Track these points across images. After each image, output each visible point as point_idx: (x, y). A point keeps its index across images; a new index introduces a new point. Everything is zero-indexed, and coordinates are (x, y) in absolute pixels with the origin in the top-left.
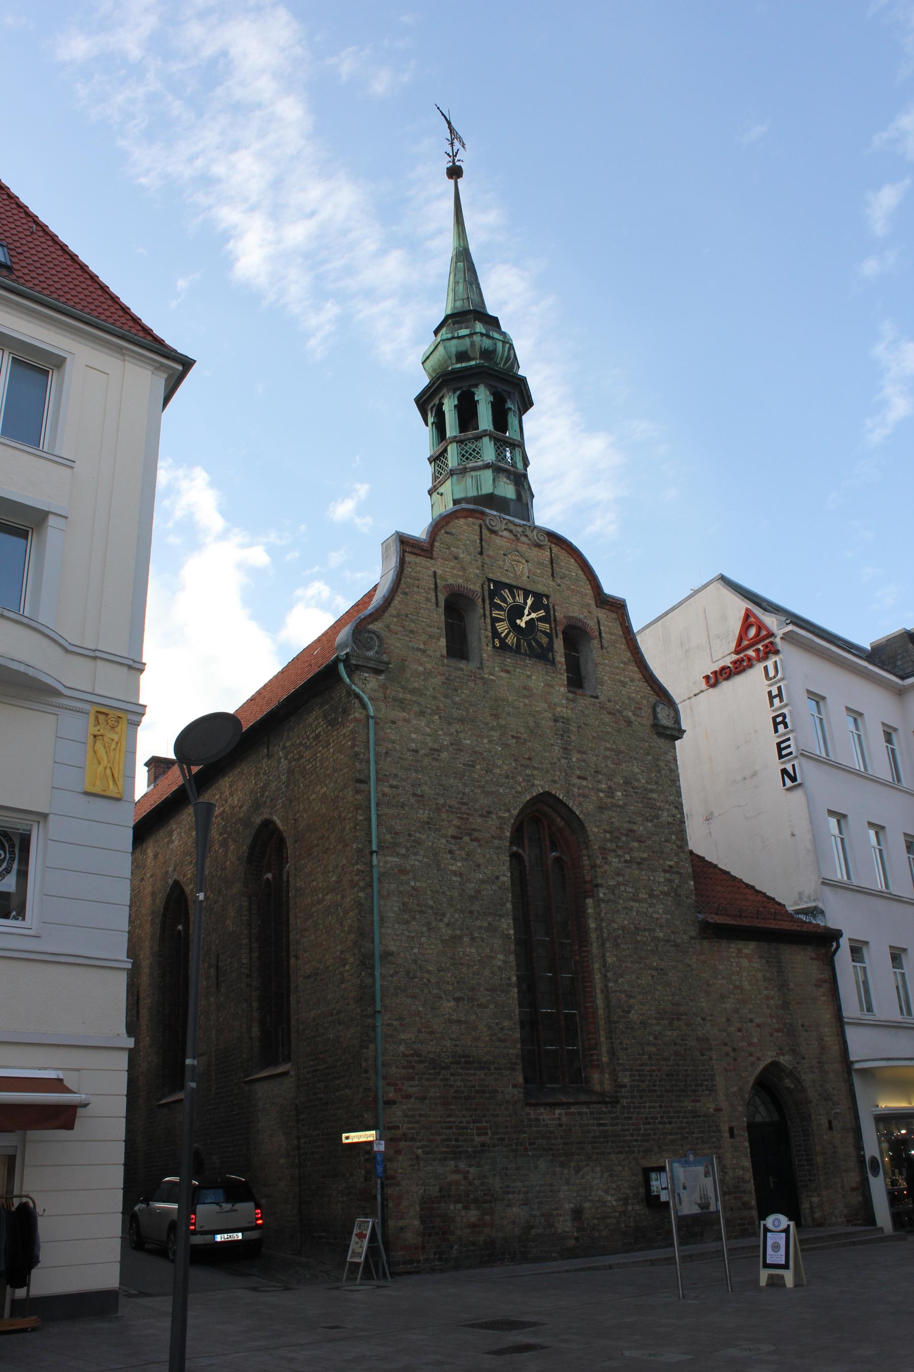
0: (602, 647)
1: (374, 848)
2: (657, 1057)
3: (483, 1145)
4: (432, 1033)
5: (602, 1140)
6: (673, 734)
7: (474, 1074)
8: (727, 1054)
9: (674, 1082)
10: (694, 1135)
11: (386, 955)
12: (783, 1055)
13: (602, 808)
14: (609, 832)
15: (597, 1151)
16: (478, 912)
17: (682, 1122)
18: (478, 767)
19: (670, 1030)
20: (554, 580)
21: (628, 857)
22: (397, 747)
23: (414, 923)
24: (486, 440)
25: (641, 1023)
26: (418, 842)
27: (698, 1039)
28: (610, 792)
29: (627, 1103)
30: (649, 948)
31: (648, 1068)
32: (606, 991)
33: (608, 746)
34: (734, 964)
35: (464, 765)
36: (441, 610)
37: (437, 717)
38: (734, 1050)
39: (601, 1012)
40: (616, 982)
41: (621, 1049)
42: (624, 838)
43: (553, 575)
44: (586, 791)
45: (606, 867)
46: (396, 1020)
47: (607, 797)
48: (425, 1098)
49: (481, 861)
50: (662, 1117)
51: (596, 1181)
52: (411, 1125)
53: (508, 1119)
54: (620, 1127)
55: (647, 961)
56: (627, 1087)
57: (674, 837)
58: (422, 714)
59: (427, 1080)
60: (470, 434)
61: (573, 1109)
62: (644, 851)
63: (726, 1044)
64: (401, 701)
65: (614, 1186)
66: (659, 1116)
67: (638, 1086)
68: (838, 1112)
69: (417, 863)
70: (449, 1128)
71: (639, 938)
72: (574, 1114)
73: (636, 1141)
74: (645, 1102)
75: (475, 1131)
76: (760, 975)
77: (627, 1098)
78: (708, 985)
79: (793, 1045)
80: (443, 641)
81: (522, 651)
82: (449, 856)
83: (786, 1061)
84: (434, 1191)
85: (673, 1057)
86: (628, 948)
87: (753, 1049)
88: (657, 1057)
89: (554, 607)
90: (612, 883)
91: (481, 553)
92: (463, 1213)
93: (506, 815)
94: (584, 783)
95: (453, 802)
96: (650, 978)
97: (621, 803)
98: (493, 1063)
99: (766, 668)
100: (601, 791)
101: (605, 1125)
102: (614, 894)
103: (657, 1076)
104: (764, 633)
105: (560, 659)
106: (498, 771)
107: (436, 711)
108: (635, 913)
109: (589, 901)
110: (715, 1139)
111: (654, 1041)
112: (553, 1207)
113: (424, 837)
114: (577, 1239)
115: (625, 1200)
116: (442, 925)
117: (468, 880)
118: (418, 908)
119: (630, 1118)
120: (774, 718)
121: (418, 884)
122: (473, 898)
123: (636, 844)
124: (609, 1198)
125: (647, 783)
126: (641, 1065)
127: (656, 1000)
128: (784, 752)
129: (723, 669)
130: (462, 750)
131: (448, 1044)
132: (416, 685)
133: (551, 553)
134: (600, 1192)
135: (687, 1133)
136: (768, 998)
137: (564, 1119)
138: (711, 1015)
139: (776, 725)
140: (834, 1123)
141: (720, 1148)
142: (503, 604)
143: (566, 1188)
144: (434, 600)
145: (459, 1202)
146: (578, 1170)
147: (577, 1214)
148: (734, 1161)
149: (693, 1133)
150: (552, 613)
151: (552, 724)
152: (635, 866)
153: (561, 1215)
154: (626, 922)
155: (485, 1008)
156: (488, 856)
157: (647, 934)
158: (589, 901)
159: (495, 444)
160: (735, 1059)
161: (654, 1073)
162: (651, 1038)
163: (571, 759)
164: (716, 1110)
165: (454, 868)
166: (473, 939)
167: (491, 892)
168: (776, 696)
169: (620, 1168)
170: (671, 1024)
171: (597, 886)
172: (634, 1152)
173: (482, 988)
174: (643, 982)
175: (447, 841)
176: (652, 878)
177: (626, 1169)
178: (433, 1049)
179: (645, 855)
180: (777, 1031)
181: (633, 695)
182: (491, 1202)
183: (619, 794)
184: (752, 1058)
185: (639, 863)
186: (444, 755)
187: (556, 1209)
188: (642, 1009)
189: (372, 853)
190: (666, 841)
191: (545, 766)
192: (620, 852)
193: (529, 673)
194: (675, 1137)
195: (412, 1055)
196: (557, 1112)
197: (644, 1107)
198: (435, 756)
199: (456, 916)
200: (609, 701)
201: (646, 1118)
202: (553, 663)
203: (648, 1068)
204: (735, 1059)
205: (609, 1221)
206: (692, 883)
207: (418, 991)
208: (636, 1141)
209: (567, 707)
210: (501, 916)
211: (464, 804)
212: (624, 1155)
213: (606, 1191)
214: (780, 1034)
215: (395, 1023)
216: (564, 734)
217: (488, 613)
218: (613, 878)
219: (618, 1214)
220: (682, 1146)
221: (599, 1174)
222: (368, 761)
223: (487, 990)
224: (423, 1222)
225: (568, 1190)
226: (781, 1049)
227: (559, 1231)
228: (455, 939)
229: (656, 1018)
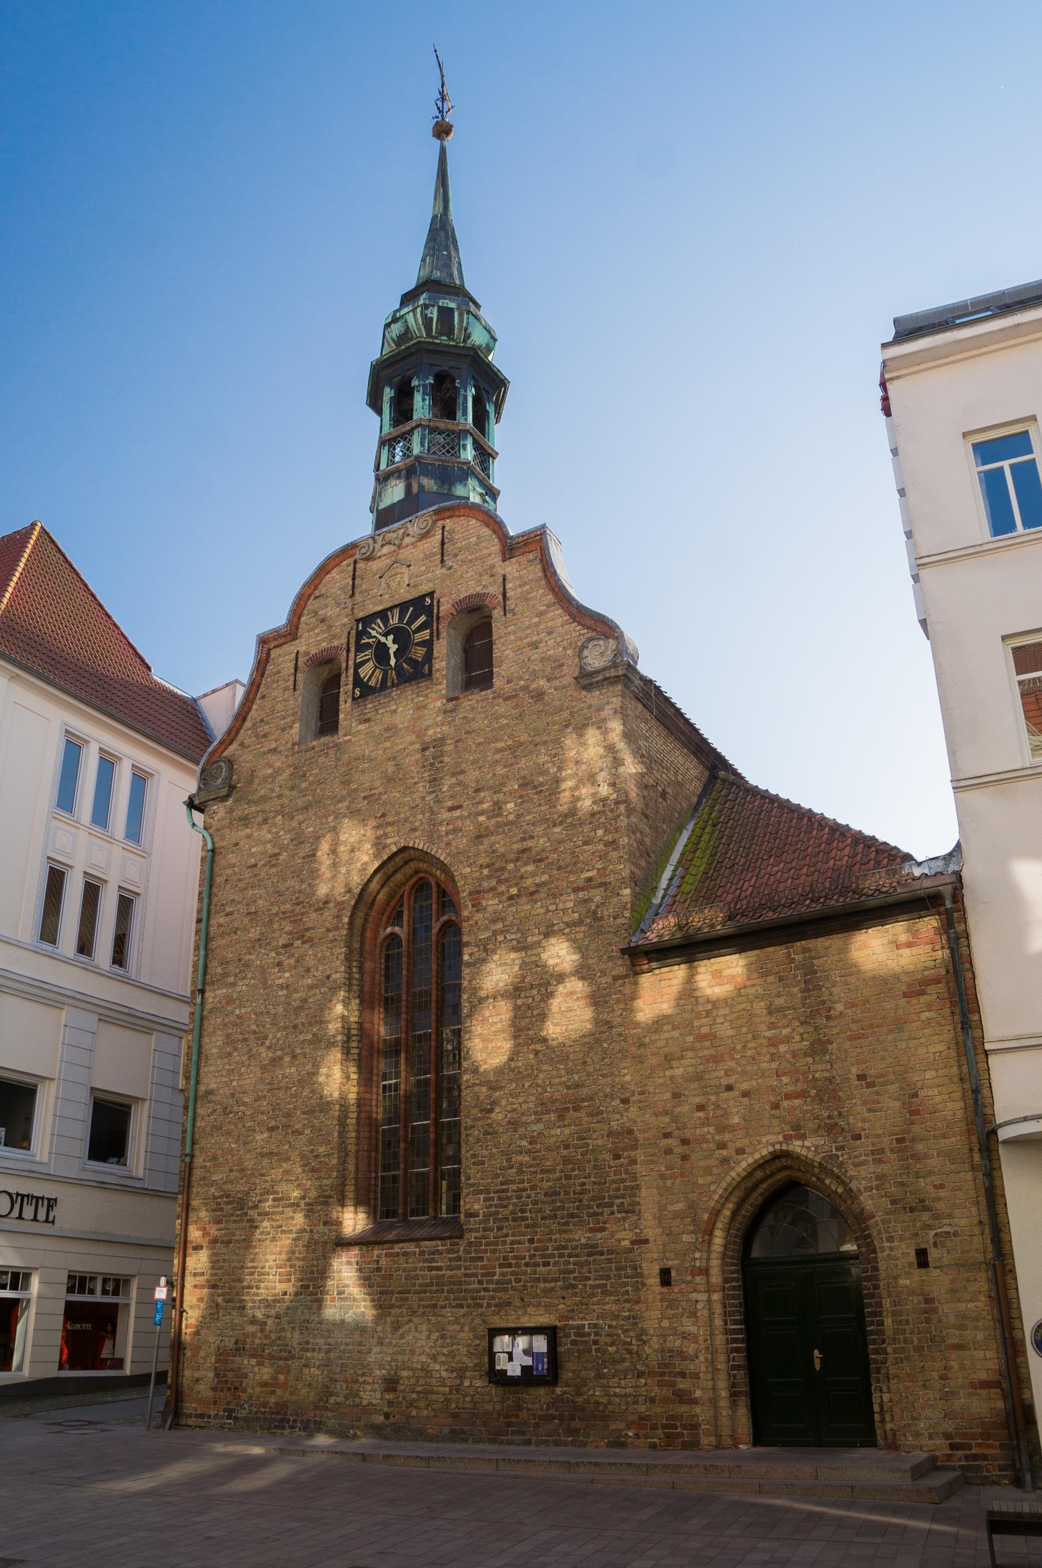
2: (532, 1169)
4: (243, 1170)
5: (435, 1288)
6: (607, 675)
7: (282, 1213)
8: (669, 1151)
9: (559, 1204)
10: (588, 1283)
12: (803, 1137)
14: (488, 866)
15: (425, 1303)
16: (303, 1024)
17: (568, 1262)
19: (559, 1127)
21: (514, 891)
23: (236, 1054)
25: (509, 1123)
26: (247, 965)
27: (610, 1134)
29: (476, 1238)
30: (535, 1012)
31: (513, 1187)
33: (500, 745)
35: (304, 858)
38: (685, 1142)
41: (474, 1164)
44: (459, 823)
45: (478, 916)
46: (210, 1160)
48: (229, 1242)
50: (532, 1256)
53: (315, 1263)
54: (463, 1271)
55: (530, 1033)
56: (478, 1216)
59: (234, 1222)
61: (397, 1249)
63: (667, 1136)
65: (445, 1351)
66: (527, 1254)
68: (948, 1233)
69: (244, 988)
72: (398, 1255)
73: (486, 1290)
74: (507, 1235)
75: (277, 1277)
76: (760, 1007)
77: (477, 1230)
78: (642, 1045)
79: (830, 1117)
82: (277, 969)
83: (808, 1148)
84: (230, 1343)
85: (559, 1168)
86: (501, 1020)
87: (727, 1137)
88: (532, 1169)
90: (483, 936)
92: (256, 1369)
96: (531, 1056)
101: (440, 1269)
103: (529, 1197)
110: (629, 1288)
111: (529, 1147)
112: (360, 1372)
113: (253, 957)
115: (461, 1372)
116: (262, 1049)
117: (296, 990)
118: (240, 1037)
119: (481, 1259)
121: (243, 1011)
122: (298, 1010)
124: (437, 1367)
126: (502, 1184)
127: (538, 1085)
130: (303, 843)
134: (424, 1358)
135: (575, 1278)
136: (773, 1042)
137: (383, 1262)
138: (642, 1093)
140: (933, 1254)
141: (637, 1302)
143: (377, 1349)
145: (253, 1356)
147: (391, 1384)
148: (665, 1323)
149: (589, 1279)
153: (368, 1383)
155: (300, 1134)
156: (319, 955)
157: (535, 992)
160: (684, 1158)
161: (524, 1194)
162: (524, 1143)
163: (440, 790)
166: (294, 1057)
167: (319, 997)
169: (457, 1327)
170: (561, 1117)
172: (481, 1306)
173: (298, 1112)
174: (520, 1064)
175: (277, 954)
177: (466, 1329)
178: (242, 1188)
179: (545, 878)
180: (788, 1096)
182: (287, 1359)
184: (724, 1152)
185: (532, 894)
187: (364, 1375)
188: (513, 1104)
192: (502, 888)
194: (552, 1284)
195: (221, 1197)
196: (376, 1252)
197: (504, 1243)
198: (274, 862)
199: (279, 1035)
201: (505, 1258)
203: (513, 1187)
204: (684, 1158)
205: (434, 1397)
207: (232, 1127)
208: (486, 1290)
211: (298, 904)
212: (466, 1309)
213: (434, 1358)
214: (797, 1102)
215: (208, 1164)
218: (487, 928)
219: (447, 1389)
220: (564, 1298)
221: (425, 1334)
223: (304, 1113)
224: (217, 1375)
225: (380, 1353)
226: (797, 1127)
227: (365, 1402)
228: (276, 1061)
229: (535, 1113)
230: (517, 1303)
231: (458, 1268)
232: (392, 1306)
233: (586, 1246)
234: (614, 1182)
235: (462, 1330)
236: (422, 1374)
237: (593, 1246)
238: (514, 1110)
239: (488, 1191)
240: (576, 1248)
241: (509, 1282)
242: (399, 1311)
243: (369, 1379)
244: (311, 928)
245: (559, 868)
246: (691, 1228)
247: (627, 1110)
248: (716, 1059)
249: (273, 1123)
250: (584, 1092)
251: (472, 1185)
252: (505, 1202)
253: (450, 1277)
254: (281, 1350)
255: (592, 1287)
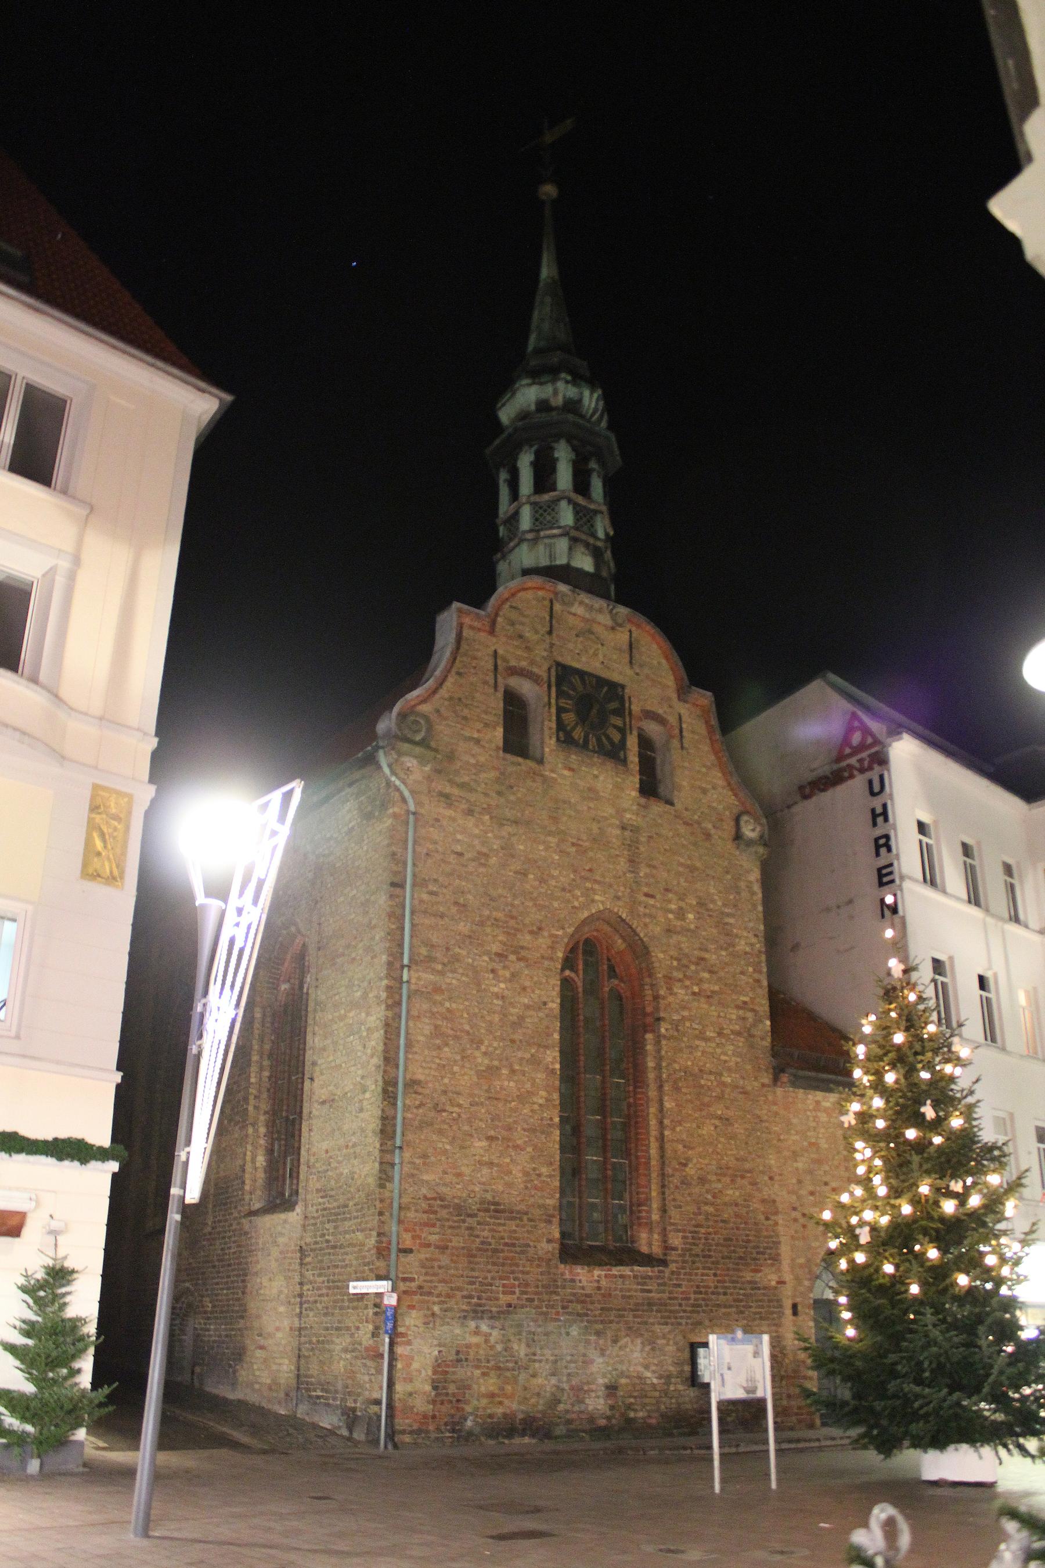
0: (682, 748)
1: (406, 961)
3: (509, 1305)
5: (645, 1308)
7: (504, 1225)
8: (795, 1220)
11: (412, 1084)
13: (669, 931)
18: (531, 876)
20: (632, 668)
21: (696, 989)
22: (440, 849)
23: (446, 1049)
24: (564, 504)
26: (457, 959)
27: (763, 1201)
28: (681, 914)
30: (714, 1094)
31: (703, 1230)
32: (661, 1138)
33: (682, 860)
34: (811, 1119)
35: (516, 872)
36: (500, 695)
37: (487, 817)
38: (804, 1215)
39: (653, 1163)
40: (673, 1129)
42: (693, 967)
43: (631, 662)
44: (654, 911)
45: (671, 999)
46: (420, 1157)
47: (677, 918)
48: (447, 1248)
49: (527, 984)
51: (636, 1355)
52: (428, 1278)
53: (540, 1277)
57: (751, 969)
58: (470, 812)
59: (451, 1227)
60: (546, 497)
62: (715, 984)
63: (794, 1209)
64: (447, 796)
67: (691, 1250)
69: (454, 981)
70: (472, 1283)
71: (703, 1082)
72: (615, 1276)
73: (685, 1311)
78: (779, 1140)
80: (499, 732)
81: (591, 747)
82: (491, 976)
89: (630, 698)
90: (676, 1017)
91: (550, 633)
93: (560, 933)
94: (651, 901)
95: (500, 915)
97: (692, 926)
98: (526, 1213)
99: (870, 782)
100: (671, 911)
101: (649, 1291)
102: (678, 1030)
104: (869, 740)
105: (633, 758)
106: (553, 883)
107: (488, 810)
108: (699, 1054)
109: (649, 1036)
113: (464, 953)
114: (608, 1418)
115: (668, 1378)
116: (477, 1054)
118: (451, 1032)
119: (679, 1286)
120: (876, 840)
121: (454, 1006)
123: (706, 975)
125: (724, 905)
127: (718, 1153)
128: (885, 880)
129: (820, 779)
131: (477, 1189)
132: (466, 779)
133: (631, 637)
135: (744, 1306)
138: (781, 1175)
139: (878, 847)
142: (571, 692)
144: (492, 682)
146: (615, 1341)
147: (612, 1389)
149: (751, 1307)
150: (627, 705)
151: (618, 832)
152: (703, 1000)
154: (689, 1063)
156: (536, 979)
157: (712, 1078)
158: (649, 1036)
159: (574, 508)
160: (804, 1226)
161: (710, 1237)
162: (709, 1197)
164: (778, 1283)
165: (496, 990)
166: (513, 1071)
167: (536, 1020)
168: (880, 815)
169: (664, 1341)
171: (659, 1019)
175: (490, 959)
176: (722, 1014)
177: (671, 1342)
178: (459, 1194)
179: (716, 988)
181: (715, 804)
182: (513, 1370)
183: (691, 916)
185: (708, 997)
186: (493, 860)
187: (588, 1383)
189: (403, 967)
190: (742, 973)
191: (607, 880)
192: (687, 983)
193: (596, 772)
195: (435, 1199)
198: (483, 861)
199: (495, 1044)
200: (686, 809)
201: (698, 1287)
202: (624, 762)
205: (647, 1401)
206: (768, 1023)
208: (685, 1311)
209: (637, 814)
210: (547, 1047)
211: (512, 917)
213: (647, 1367)
215: (417, 1161)
216: (632, 846)
217: (553, 701)
222: (405, 863)
223: (524, 1130)
224: (435, 1388)
227: (590, 1408)
228: (492, 1071)
229: (716, 1174)
230: (707, 1323)
231: (664, 1292)
232: (611, 1322)
233: (750, 1282)
234: (766, 1237)
235: (668, 1345)
236: (637, 1381)
237: (756, 1283)
238: (702, 1169)
239: (684, 1231)
240: (743, 1283)
241: (700, 1306)
242: (618, 1326)
243: (593, 1387)
244: (528, 949)
245: (726, 985)
246: (808, 1276)
247: (773, 1185)
248: (819, 1162)
249: (492, 1133)
250: (747, 1166)
251: (674, 1224)
252: (697, 1242)
253: (659, 1299)
254: (507, 1361)
255: (755, 1313)
